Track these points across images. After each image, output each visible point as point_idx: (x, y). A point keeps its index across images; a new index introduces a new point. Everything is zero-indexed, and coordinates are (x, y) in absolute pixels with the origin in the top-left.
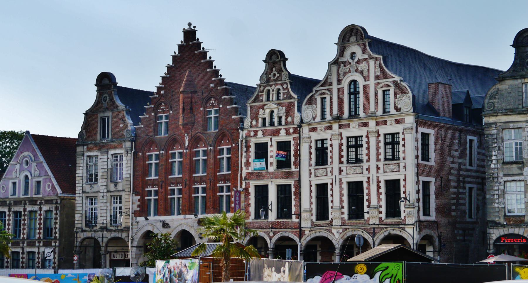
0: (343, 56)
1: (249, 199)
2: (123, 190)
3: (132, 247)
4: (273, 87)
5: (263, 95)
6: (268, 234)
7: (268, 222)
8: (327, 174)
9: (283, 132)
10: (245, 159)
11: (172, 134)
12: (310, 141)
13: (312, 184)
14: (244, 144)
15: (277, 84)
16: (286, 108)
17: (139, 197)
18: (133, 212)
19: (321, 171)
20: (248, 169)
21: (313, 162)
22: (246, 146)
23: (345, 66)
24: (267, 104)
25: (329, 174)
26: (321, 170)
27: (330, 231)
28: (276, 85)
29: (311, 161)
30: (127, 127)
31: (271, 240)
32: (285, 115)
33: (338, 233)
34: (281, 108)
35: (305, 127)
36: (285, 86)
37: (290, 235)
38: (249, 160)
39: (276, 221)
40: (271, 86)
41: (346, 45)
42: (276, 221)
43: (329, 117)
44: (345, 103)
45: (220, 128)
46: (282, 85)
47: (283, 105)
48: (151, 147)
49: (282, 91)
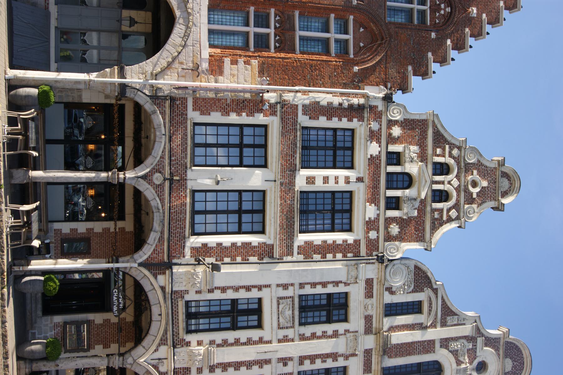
0: (486, 345)
4: (455, 183)
6: (158, 169)
7: (186, 167)
8: (282, 328)
9: (371, 211)
12: (349, 282)
13: (264, 290)
14: (355, 101)
16: (414, 217)
19: (288, 313)
21: (308, 290)
22: (351, 106)
23: (468, 350)
25: (282, 333)
26: (291, 312)
27: (163, 342)
28: (458, 189)
29: (309, 286)
31: (144, 177)
32: (405, 217)
33: (157, 361)
34: (417, 204)
35: (376, 271)
36: (454, 214)
37: (156, 234)
38: (323, 115)
39: (188, 191)
41: (501, 352)
42: (188, 191)
43: (388, 322)
44: (408, 357)
46: (456, 206)
47: (421, 210)
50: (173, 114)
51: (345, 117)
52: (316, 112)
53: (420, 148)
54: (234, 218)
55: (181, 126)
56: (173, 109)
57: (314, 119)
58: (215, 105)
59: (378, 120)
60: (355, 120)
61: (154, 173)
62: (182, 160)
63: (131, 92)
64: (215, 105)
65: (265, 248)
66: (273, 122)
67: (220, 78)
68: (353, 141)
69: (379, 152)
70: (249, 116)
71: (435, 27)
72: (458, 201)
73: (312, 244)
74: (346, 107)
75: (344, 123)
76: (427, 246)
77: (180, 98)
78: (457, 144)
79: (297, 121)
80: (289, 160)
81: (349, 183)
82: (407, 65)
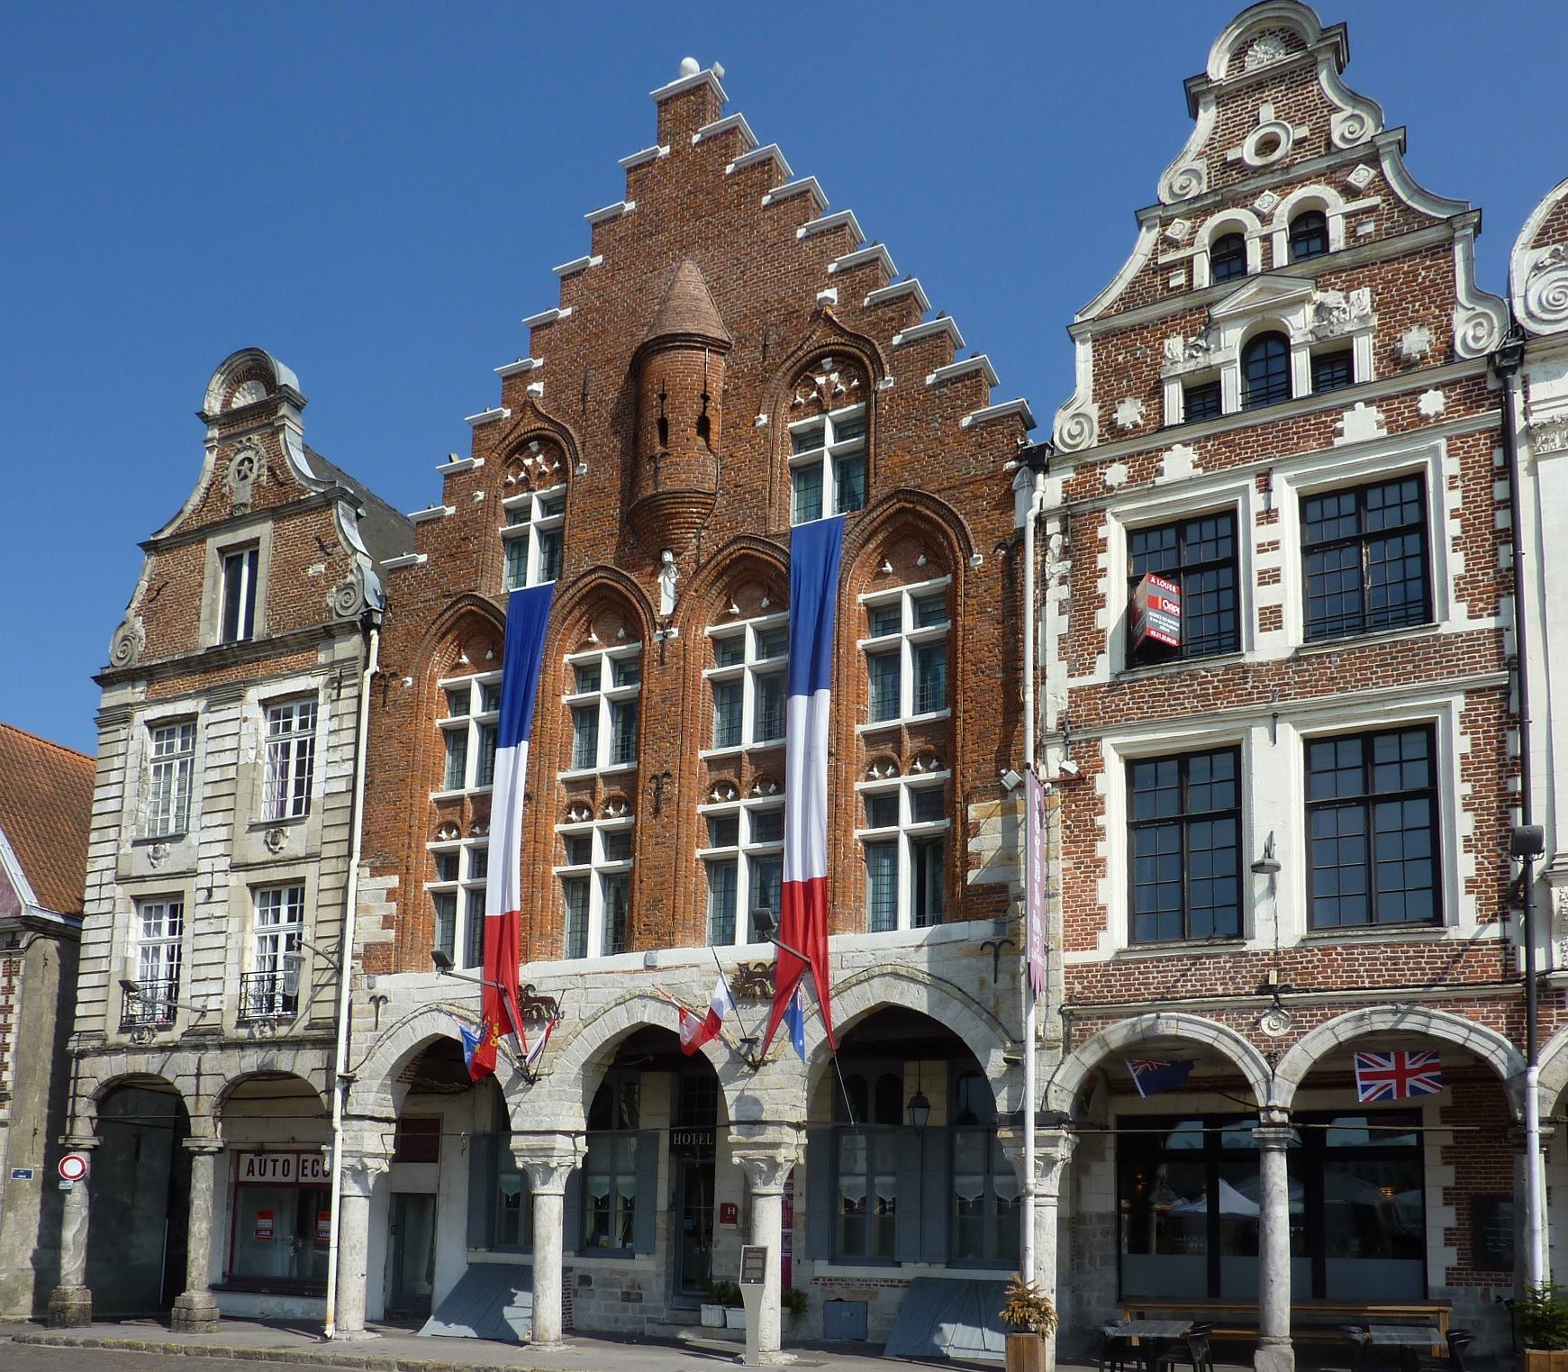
4: (1265, 202)
16: (1374, 292)
28: (1283, 188)
40: (1244, 200)
46: (1333, 176)
49: (1337, 209)
50: (1107, 997)
51: (1095, 562)
53: (1168, 337)
54: (1387, 816)
55: (1137, 975)
58: (1080, 896)
60: (1101, 532)
64: (1080, 896)
65: (1476, 715)
70: (1103, 808)
72: (1318, 176)
73: (1461, 578)
74: (1069, 564)
76: (1463, 227)
77: (1066, 983)
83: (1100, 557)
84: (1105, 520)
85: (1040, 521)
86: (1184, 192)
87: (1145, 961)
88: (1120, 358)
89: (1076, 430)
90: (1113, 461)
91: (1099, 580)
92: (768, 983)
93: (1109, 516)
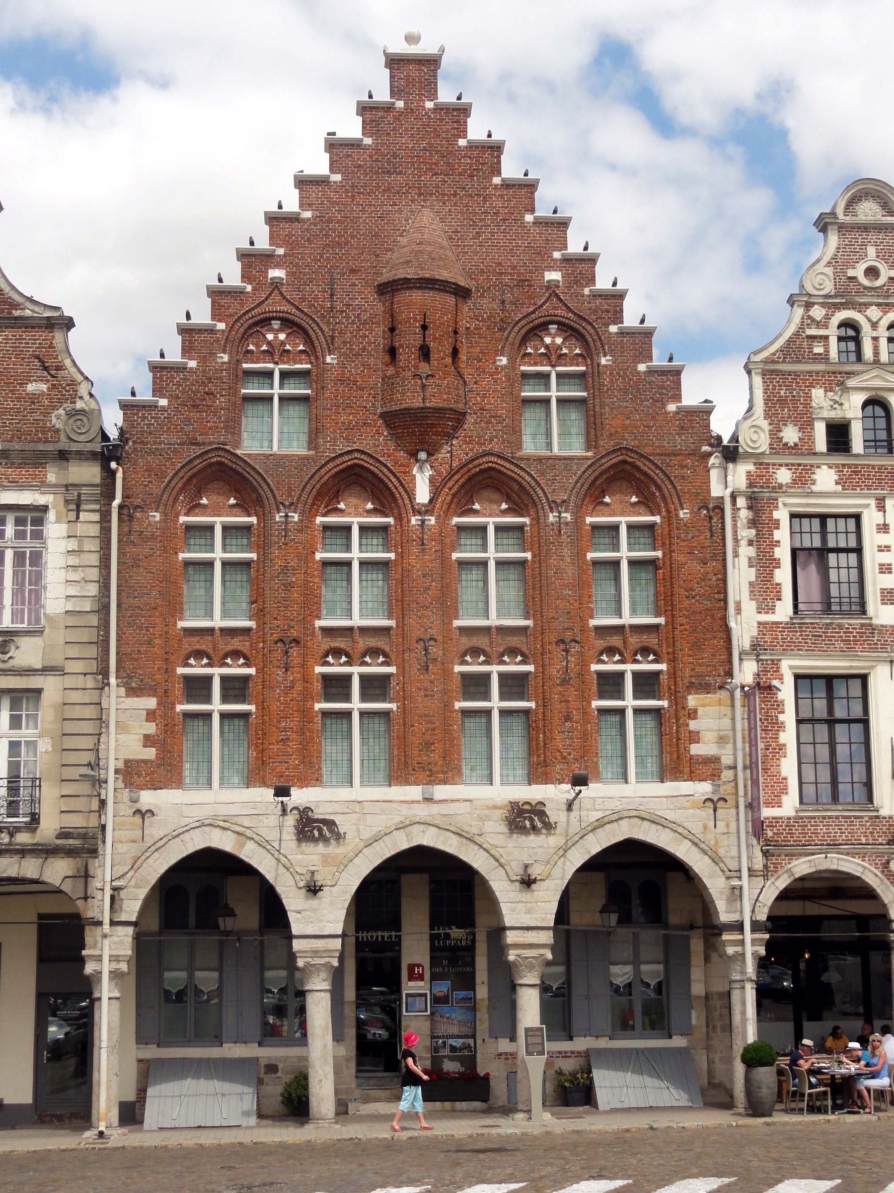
1: (781, 726)
2: (46, 670)
3: (113, 923)
5: (826, 338)
7: (877, 817)
10: (753, 570)
11: (341, 447)
15: (887, 305)
17: (151, 703)
18: (121, 765)
20: (766, 607)
22: (753, 523)
24: (863, 372)
30: (74, 397)
38: (771, 574)
40: (862, 307)
45: (606, 444)
48: (199, 494)
51: (772, 535)
52: (768, 588)
53: (814, 387)
56: (782, 841)
57: (780, 592)
59: (771, 470)
60: (776, 515)
61: (890, 871)
62: (865, 825)
63: (760, 912)
66: (791, 667)
67: (726, 760)
68: (810, 516)
69: (830, 467)
71: (588, 355)
74: (753, 532)
75: (782, 535)
78: (799, 312)
79: (787, 623)
80: (855, 637)
81: (888, 525)
82: (667, 413)
83: (776, 532)
84: (777, 507)
85: (733, 497)
86: (822, 287)
87: (814, 818)
88: (782, 393)
89: (755, 437)
90: (781, 465)
91: (776, 548)
92: (536, 818)
93: (780, 505)
